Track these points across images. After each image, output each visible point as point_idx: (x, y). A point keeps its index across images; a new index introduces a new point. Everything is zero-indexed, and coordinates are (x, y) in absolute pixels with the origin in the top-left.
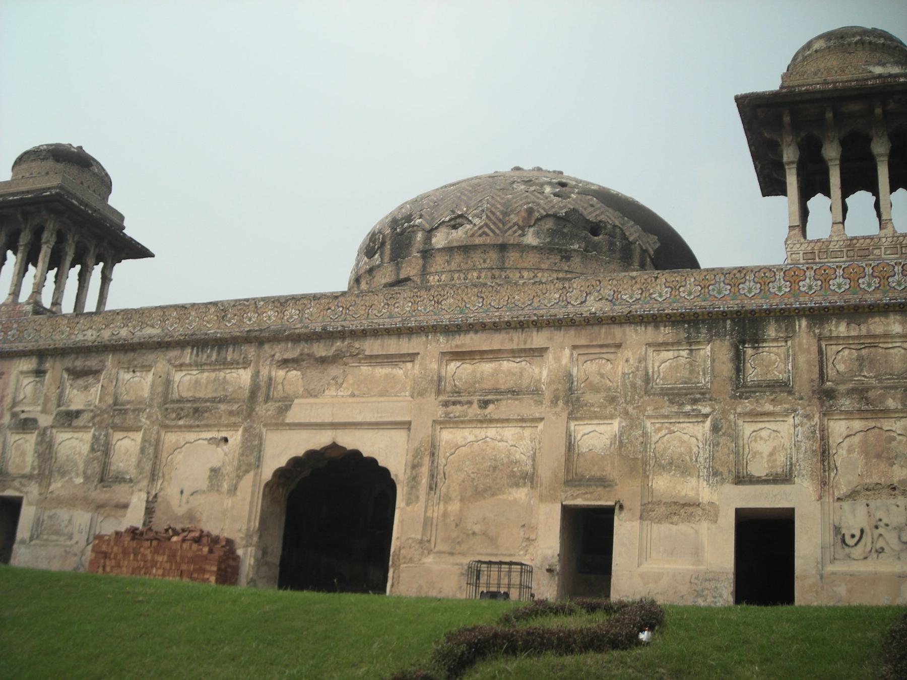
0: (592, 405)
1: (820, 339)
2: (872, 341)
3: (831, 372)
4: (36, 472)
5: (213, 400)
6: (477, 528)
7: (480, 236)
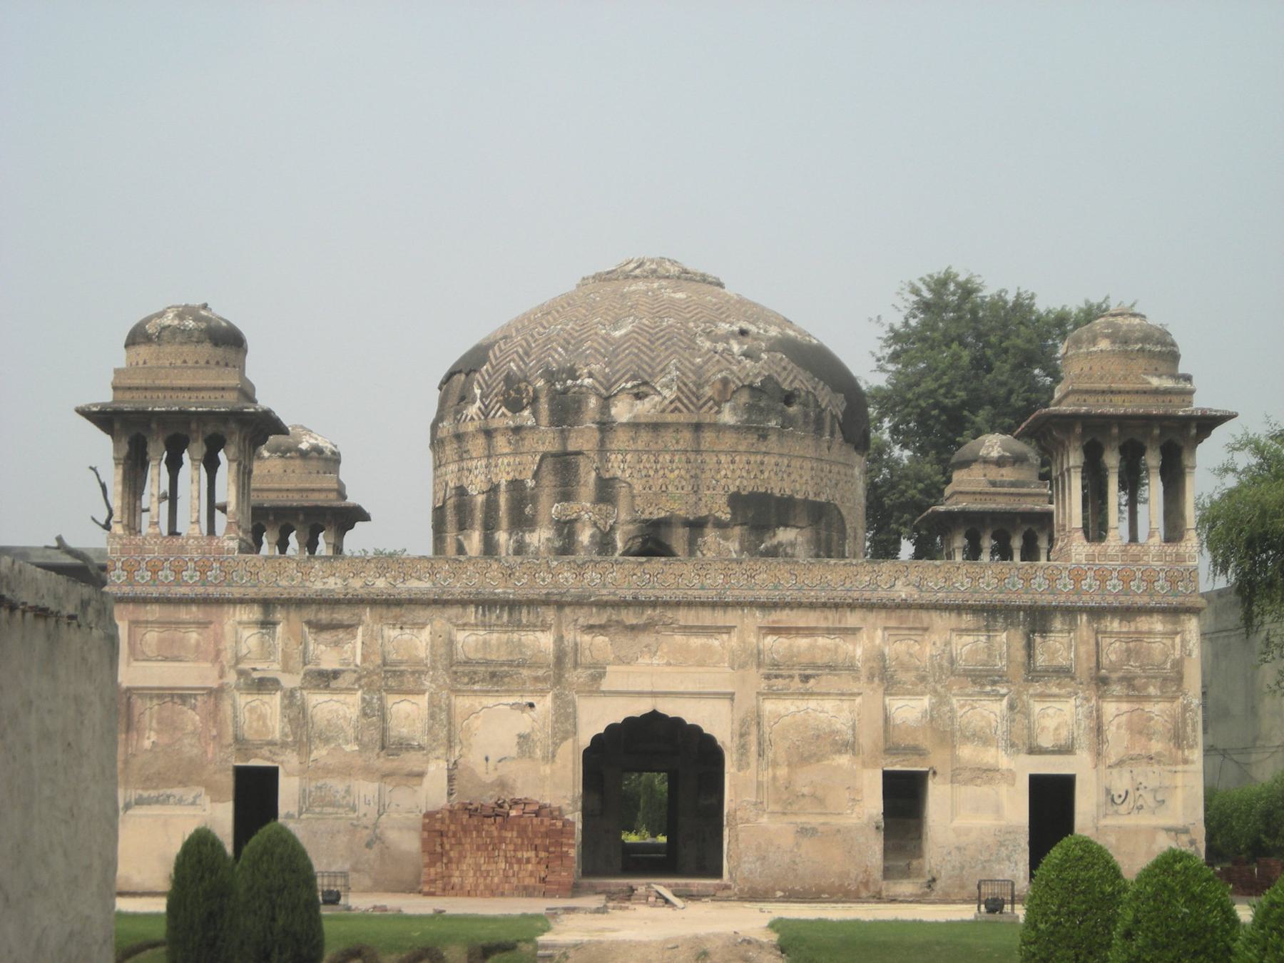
0: (905, 683)
1: (1097, 633)
2: (1139, 636)
3: (1105, 661)
4: (290, 739)
5: (510, 663)
6: (806, 790)
7: (672, 411)
